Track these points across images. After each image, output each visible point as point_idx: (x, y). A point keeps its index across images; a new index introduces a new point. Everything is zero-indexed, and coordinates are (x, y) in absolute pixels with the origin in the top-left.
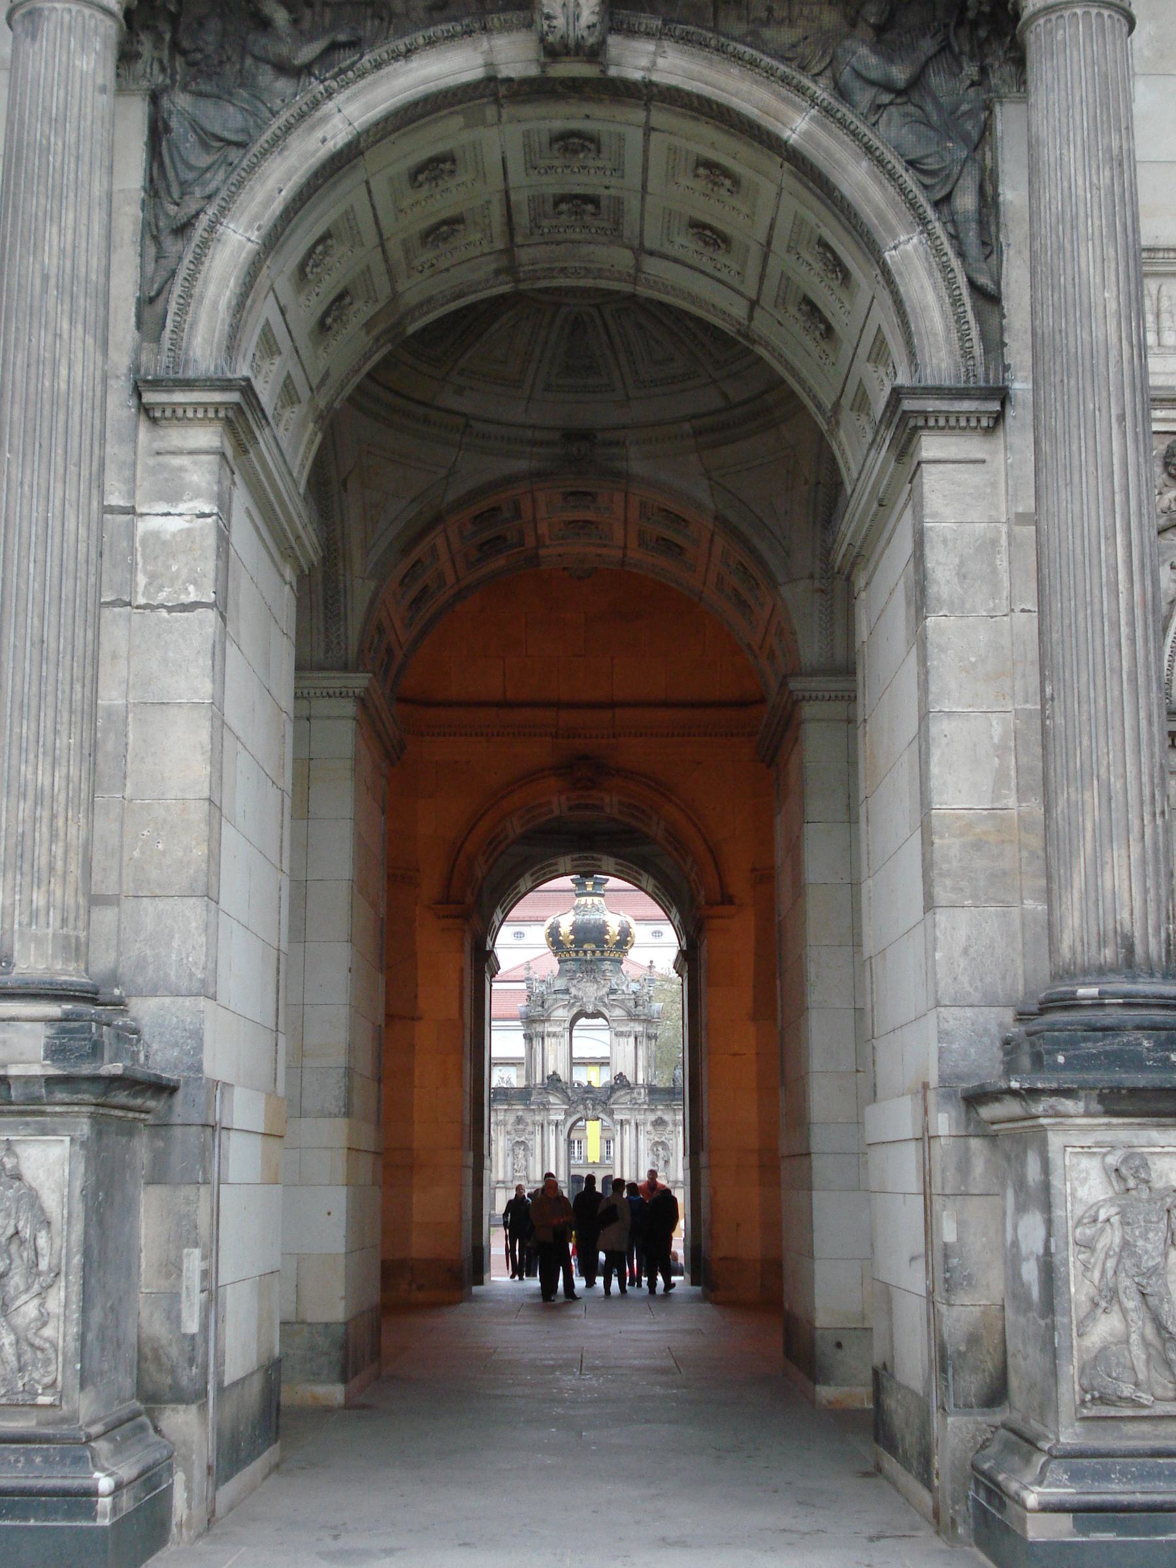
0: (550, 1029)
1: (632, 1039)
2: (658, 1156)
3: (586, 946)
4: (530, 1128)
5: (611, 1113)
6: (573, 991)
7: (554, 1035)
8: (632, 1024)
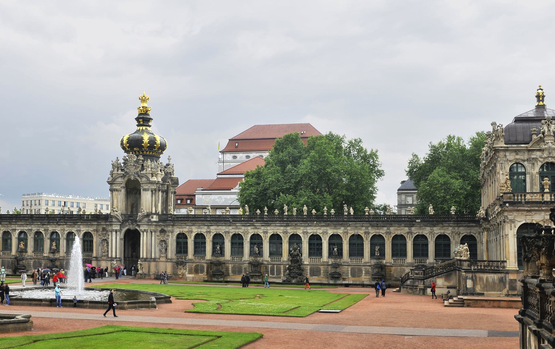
3: (135, 149)
6: (125, 169)
7: (117, 190)
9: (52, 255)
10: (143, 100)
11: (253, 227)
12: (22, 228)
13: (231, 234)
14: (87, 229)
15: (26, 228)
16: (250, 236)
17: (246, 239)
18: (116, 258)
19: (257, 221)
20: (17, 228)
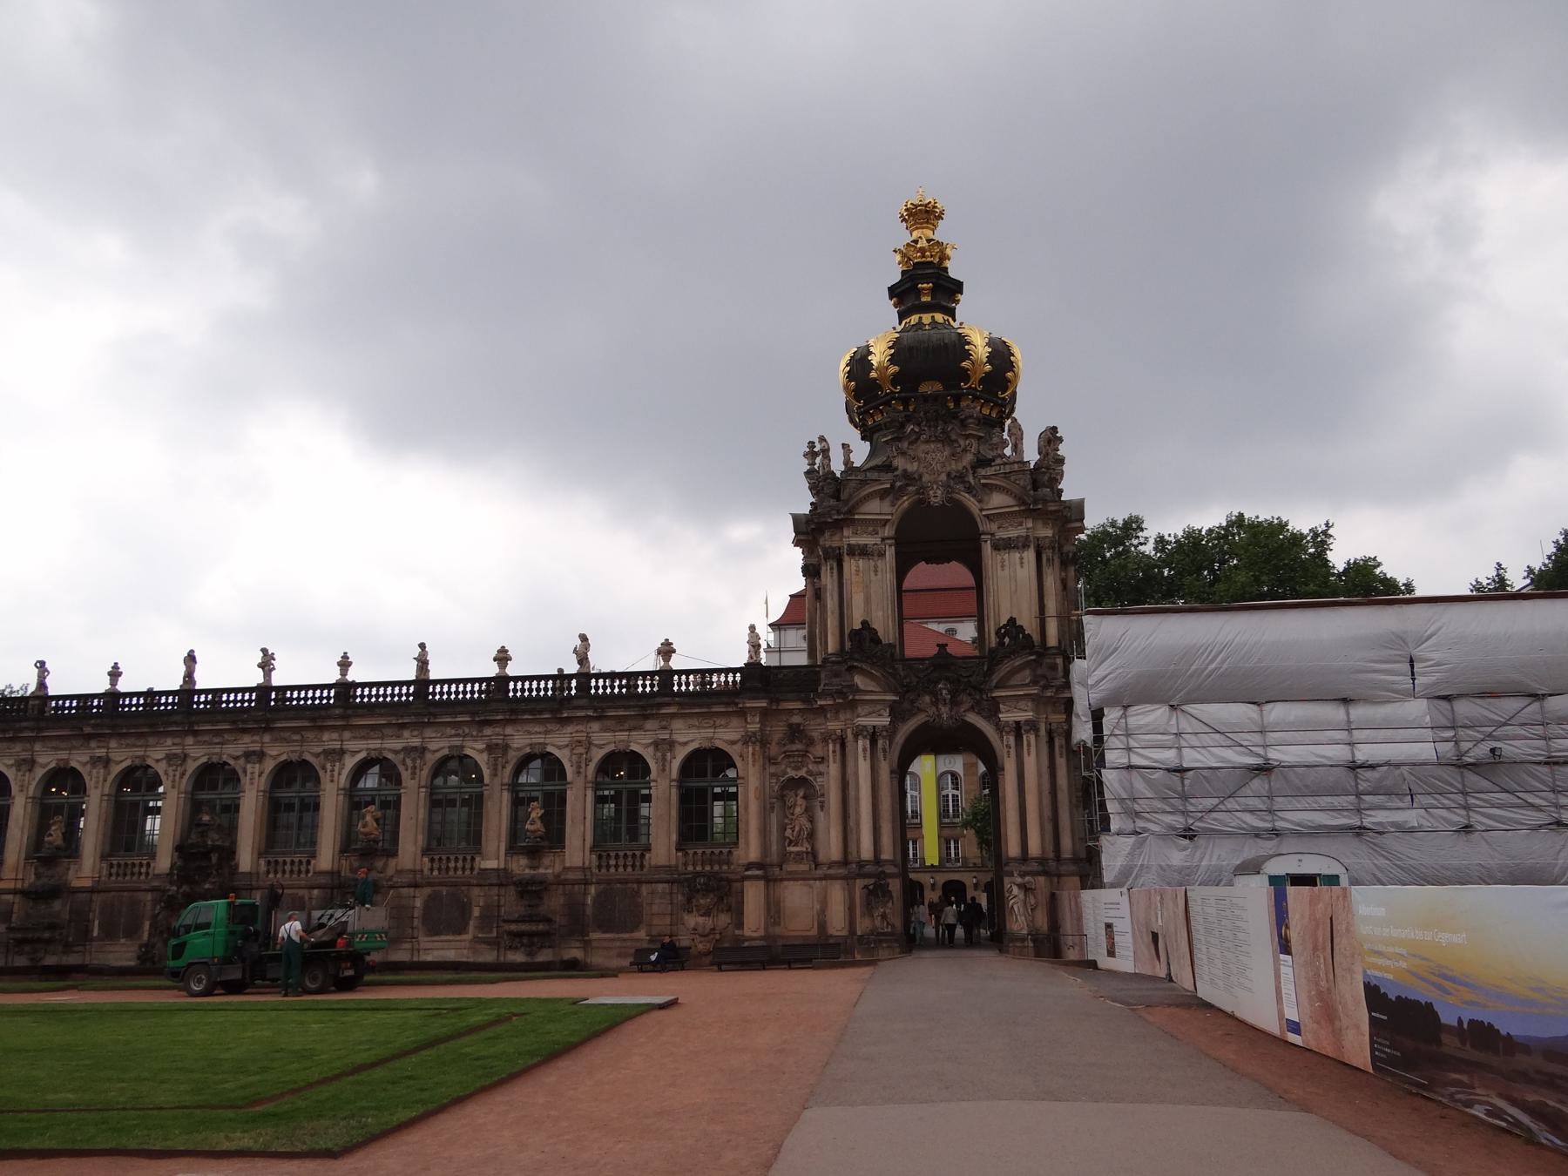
0: (853, 541)
1: (1030, 555)
4: (818, 750)
5: (992, 713)
7: (862, 552)
9: (523, 861)
12: (375, 744)
14: (709, 733)
15: (397, 744)
20: (351, 745)
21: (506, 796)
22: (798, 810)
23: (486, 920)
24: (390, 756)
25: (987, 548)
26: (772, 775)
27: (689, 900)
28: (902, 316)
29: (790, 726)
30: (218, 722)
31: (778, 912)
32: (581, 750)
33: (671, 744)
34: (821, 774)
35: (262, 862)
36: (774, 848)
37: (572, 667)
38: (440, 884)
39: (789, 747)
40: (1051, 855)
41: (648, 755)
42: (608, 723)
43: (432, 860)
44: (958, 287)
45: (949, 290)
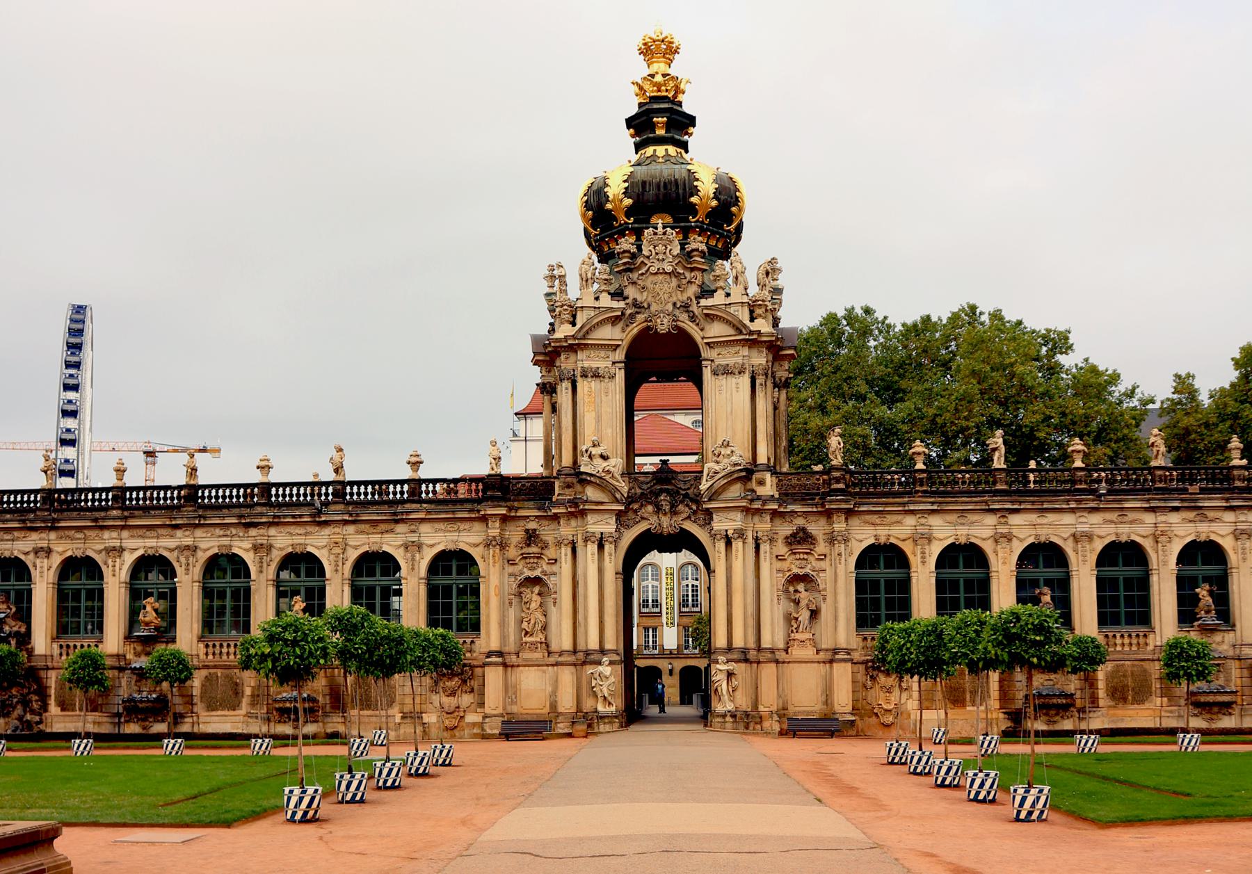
0: (586, 364)
1: (745, 380)
2: (797, 602)
4: (551, 553)
6: (631, 292)
7: (596, 375)
8: (745, 351)
10: (659, 49)
11: (1191, 515)
12: (151, 543)
13: (1099, 546)
14: (453, 536)
15: (171, 543)
16: (1177, 547)
17: (1165, 563)
18: (602, 651)
19: (1203, 491)
20: (129, 543)
21: (272, 592)
22: (533, 605)
23: (255, 698)
24: (166, 554)
25: (707, 373)
26: (510, 575)
27: (436, 683)
28: (638, 147)
29: (527, 531)
30: (7, 521)
31: (515, 693)
32: (338, 550)
33: (419, 546)
34: (555, 574)
35: (55, 646)
36: (512, 638)
37: (329, 476)
38: (215, 667)
39: (526, 550)
40: (752, 644)
41: (399, 555)
42: (362, 527)
43: (207, 646)
44: (691, 121)
45: (682, 123)
